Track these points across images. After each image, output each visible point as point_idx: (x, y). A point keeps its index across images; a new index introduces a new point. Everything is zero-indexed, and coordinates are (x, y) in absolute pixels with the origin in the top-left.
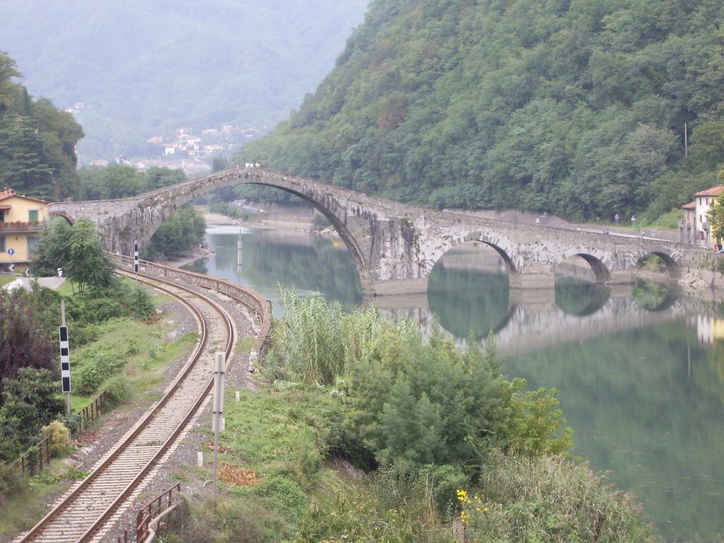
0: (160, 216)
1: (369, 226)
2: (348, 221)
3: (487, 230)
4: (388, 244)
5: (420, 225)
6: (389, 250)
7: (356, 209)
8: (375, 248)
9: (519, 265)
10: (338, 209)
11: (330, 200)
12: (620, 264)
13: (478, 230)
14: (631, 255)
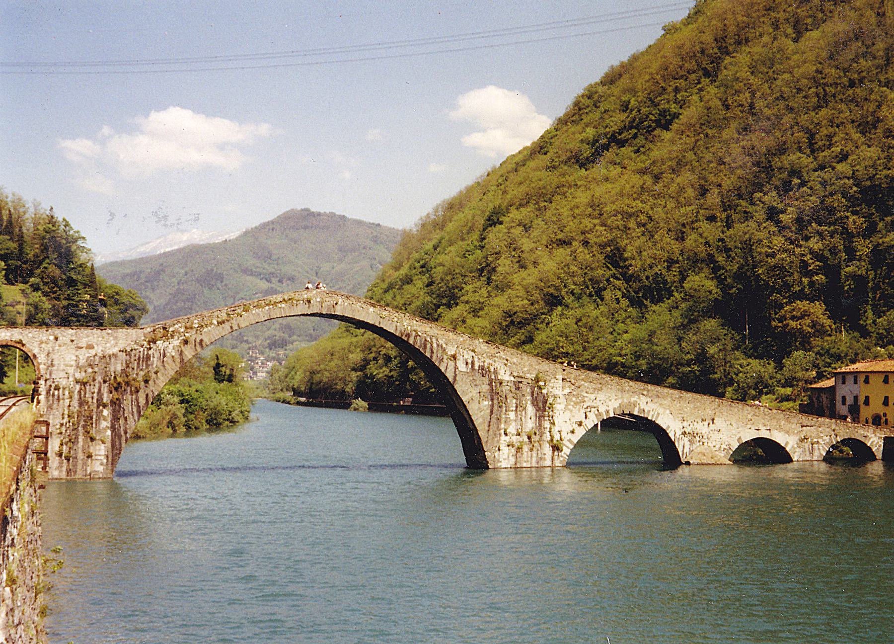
0: (177, 356)
1: (488, 387)
2: (457, 378)
4: (512, 415)
6: (513, 424)
7: (470, 361)
10: (445, 360)
12: (807, 453)
13: (633, 400)
14: (820, 440)
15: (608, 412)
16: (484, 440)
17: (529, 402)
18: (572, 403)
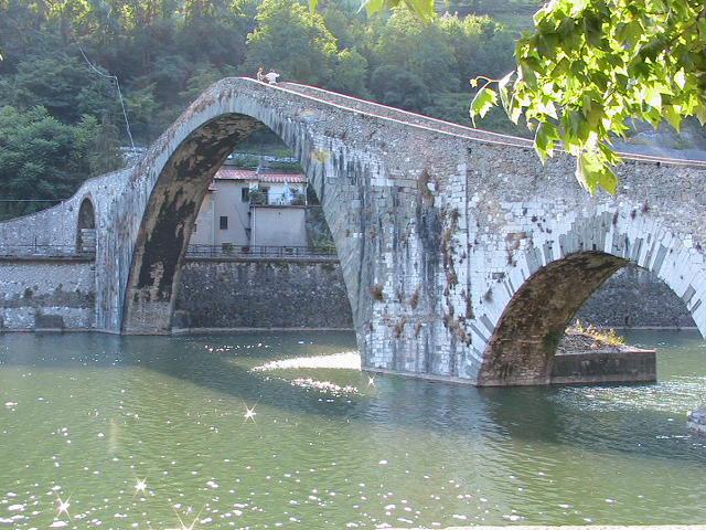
5: (454, 196)
6: (390, 278)
8: (365, 270)
11: (303, 137)
15: (548, 246)
16: (354, 309)
18: (487, 229)
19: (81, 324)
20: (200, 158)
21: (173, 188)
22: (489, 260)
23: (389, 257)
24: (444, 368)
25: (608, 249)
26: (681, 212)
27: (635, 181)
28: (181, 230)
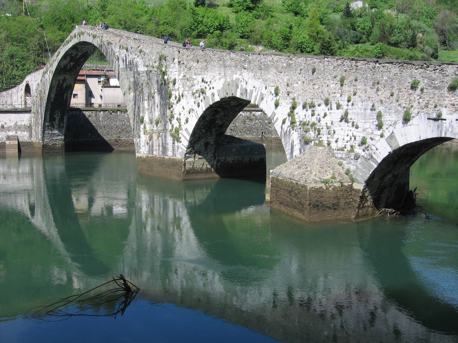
2: (120, 75)
3: (247, 75)
6: (147, 113)
8: (137, 109)
9: (292, 152)
11: (110, 49)
13: (235, 77)
17: (156, 91)
18: (187, 88)
19: (26, 139)
20: (72, 64)
21: (61, 78)
22: (188, 103)
23: (146, 103)
24: (170, 153)
25: (238, 95)
26: (269, 76)
27: (249, 62)
28: (67, 96)
